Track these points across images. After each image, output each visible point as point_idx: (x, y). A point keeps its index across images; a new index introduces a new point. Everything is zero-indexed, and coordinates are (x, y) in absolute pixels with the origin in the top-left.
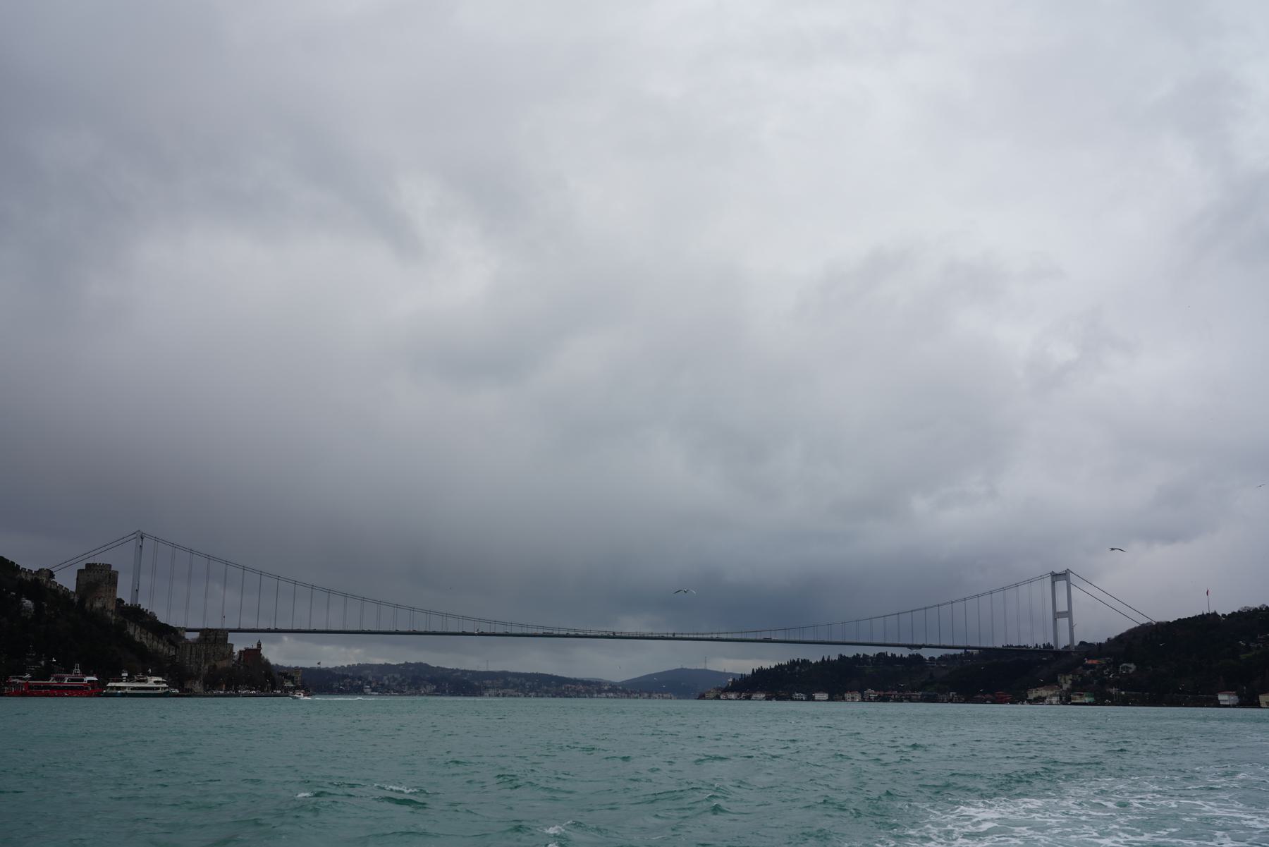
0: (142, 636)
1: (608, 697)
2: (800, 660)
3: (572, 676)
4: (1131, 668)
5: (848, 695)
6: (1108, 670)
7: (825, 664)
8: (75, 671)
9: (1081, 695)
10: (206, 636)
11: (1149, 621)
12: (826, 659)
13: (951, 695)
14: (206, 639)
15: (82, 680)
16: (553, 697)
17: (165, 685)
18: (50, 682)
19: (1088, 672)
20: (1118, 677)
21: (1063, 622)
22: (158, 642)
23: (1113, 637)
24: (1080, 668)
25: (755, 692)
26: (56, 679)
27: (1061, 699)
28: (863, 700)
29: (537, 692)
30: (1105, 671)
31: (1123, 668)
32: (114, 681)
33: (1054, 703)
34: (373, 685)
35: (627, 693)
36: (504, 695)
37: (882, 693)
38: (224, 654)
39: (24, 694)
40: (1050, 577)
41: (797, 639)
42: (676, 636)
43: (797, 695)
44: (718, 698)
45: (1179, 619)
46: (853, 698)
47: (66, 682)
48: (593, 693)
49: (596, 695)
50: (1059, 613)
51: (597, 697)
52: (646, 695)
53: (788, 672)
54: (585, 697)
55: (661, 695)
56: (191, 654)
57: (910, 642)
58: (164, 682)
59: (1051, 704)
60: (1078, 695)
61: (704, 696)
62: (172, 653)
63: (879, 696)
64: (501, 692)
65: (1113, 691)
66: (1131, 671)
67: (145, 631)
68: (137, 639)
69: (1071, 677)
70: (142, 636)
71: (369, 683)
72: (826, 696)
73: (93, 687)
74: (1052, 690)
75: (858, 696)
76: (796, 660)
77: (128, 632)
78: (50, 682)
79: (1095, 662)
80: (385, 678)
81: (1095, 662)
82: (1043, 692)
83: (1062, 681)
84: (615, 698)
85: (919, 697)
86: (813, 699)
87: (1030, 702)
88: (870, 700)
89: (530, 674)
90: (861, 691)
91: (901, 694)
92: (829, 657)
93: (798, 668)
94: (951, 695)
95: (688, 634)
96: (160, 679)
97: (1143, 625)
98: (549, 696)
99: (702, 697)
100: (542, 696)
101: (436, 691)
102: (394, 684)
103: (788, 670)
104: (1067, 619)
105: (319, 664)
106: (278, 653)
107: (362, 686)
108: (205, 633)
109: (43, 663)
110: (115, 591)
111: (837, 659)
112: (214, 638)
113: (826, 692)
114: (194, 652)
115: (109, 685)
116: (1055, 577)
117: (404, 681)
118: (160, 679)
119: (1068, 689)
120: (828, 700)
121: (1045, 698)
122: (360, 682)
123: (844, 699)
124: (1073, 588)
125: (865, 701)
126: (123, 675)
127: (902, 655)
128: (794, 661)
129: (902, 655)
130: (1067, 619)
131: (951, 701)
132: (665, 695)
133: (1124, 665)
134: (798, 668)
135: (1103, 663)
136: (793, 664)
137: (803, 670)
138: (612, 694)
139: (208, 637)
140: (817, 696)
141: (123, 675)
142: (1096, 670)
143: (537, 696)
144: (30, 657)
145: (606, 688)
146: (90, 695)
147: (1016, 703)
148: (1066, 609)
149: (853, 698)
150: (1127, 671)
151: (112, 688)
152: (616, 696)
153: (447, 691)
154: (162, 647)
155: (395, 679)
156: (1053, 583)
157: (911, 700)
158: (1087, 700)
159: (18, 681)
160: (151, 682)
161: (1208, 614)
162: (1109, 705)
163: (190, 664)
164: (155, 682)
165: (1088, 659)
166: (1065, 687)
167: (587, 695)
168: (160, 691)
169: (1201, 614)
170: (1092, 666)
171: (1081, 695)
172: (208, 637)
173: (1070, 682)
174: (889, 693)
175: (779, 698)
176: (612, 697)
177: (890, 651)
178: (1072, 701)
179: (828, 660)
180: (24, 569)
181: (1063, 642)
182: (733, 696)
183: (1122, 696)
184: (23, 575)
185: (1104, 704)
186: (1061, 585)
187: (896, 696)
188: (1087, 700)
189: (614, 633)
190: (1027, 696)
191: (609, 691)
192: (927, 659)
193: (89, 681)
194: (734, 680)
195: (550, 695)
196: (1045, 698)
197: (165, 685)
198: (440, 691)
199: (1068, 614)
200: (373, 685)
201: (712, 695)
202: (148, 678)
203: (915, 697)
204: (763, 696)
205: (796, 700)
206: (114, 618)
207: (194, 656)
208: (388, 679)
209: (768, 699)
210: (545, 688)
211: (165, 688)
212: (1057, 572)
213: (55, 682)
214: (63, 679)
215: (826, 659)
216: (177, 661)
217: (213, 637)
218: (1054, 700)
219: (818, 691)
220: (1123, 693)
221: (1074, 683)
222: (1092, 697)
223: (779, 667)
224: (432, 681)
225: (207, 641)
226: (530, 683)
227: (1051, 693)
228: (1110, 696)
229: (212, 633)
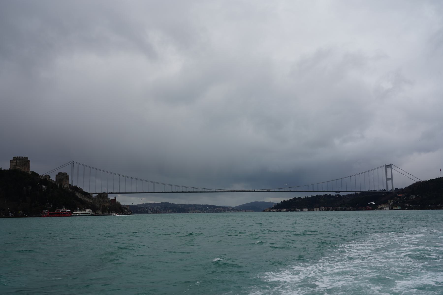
0: (81, 196)
1: (231, 212)
2: (298, 198)
3: (218, 205)
4: (413, 197)
5: (315, 209)
6: (406, 198)
7: (307, 199)
8: (63, 208)
9: (396, 206)
11: (420, 180)
12: (307, 197)
13: (351, 208)
14: (100, 197)
15: (66, 211)
16: (212, 212)
17: (92, 212)
18: (55, 212)
19: (399, 199)
20: (409, 200)
21: (390, 182)
22: (86, 198)
23: (407, 186)
24: (396, 197)
25: (283, 209)
26: (57, 211)
27: (389, 208)
28: (320, 210)
29: (207, 211)
30: (404, 198)
31: (411, 197)
32: (75, 211)
33: (387, 209)
34: (151, 210)
36: (196, 212)
37: (327, 208)
38: (107, 201)
39: (48, 216)
40: (385, 167)
41: (297, 190)
43: (297, 209)
44: (270, 211)
45: (431, 180)
46: (316, 210)
47: (61, 212)
48: (226, 211)
49: (227, 211)
50: (388, 179)
51: (227, 212)
52: (244, 211)
53: (294, 202)
54: (223, 212)
55: (249, 211)
56: (97, 202)
57: (336, 191)
58: (91, 211)
59: (386, 210)
60: (395, 206)
61: (265, 210)
62: (91, 201)
63: (326, 209)
64: (194, 211)
65: (408, 205)
66: (414, 198)
67: (81, 195)
68: (79, 197)
69: (393, 200)
70: (81, 196)
71: (150, 210)
72: (307, 210)
73: (69, 214)
74: (386, 205)
75: (318, 209)
76: (296, 198)
77: (76, 195)
78: (55, 212)
79: (401, 195)
80: (155, 208)
81: (401, 195)
82: (383, 206)
83: (390, 202)
84: (234, 212)
85: (340, 209)
86: (303, 211)
87: (379, 209)
88: (323, 211)
89: (204, 205)
90: (319, 207)
91: (333, 208)
92: (308, 196)
93: (297, 200)
94: (351, 208)
95: (260, 190)
96: (90, 210)
97: (418, 182)
98: (211, 212)
99: (264, 211)
100: (209, 212)
101: (173, 211)
102: (159, 209)
103: (294, 201)
104: (391, 181)
105: (132, 203)
106: (123, 200)
107: (147, 211)
108: (100, 194)
109: (51, 206)
110: (68, 182)
111: (310, 197)
112: (103, 196)
113: (307, 208)
115: (74, 212)
116: (387, 166)
117: (161, 208)
118: (90, 210)
119: (392, 205)
120: (308, 211)
121: (384, 208)
122: (147, 209)
123: (313, 210)
124: (393, 170)
125: (320, 211)
126: (78, 209)
127: (333, 195)
128: (295, 198)
129: (333, 195)
130: (391, 181)
131: (350, 210)
132: (251, 211)
133: (411, 196)
134: (297, 200)
135: (404, 195)
136: (295, 199)
137: (299, 201)
138: (232, 211)
139: (101, 196)
140: (304, 210)
141: (78, 209)
142: (401, 198)
143: (207, 212)
144: (47, 204)
146: (68, 216)
147: (373, 210)
148: (391, 178)
149: (316, 210)
150: (412, 198)
151: (75, 213)
152: (234, 211)
153: (176, 211)
154: (87, 200)
155: (158, 208)
156: (386, 168)
157: (336, 210)
158: (398, 208)
159: (46, 212)
160: (87, 211)
161: (441, 177)
162: (406, 210)
163: (97, 205)
164: (89, 211)
165: (399, 195)
166: (391, 204)
167: (224, 212)
168: (90, 214)
169: (438, 177)
170: (400, 197)
171: (396, 206)
172: (101, 196)
173: (392, 202)
174: (329, 208)
175: (291, 211)
176: (232, 212)
177: (329, 194)
178: (393, 209)
179: (308, 197)
180: (41, 175)
181: (390, 188)
182: (275, 210)
183: (411, 206)
184: (40, 177)
185: (404, 210)
186: (389, 169)
187: (332, 209)
188: (398, 208)
189: (234, 190)
190: (377, 208)
191: (232, 210)
192: (342, 196)
193: (68, 211)
194: (275, 205)
195: (211, 212)
196: (384, 208)
197: (92, 212)
198: (174, 212)
199: (391, 179)
200: (151, 210)
201: (268, 210)
202: (86, 210)
203: (338, 209)
204: (285, 210)
205: (297, 211)
206: (71, 190)
208: (156, 208)
209: (287, 211)
211: (92, 213)
212: (387, 164)
213: (57, 212)
214: (60, 211)
215: (307, 197)
216: (93, 204)
217: (103, 196)
218: (387, 208)
219: (304, 208)
220: (411, 205)
221: (394, 203)
222: (400, 207)
223: (291, 200)
224: (171, 208)
226: (204, 208)
227: (386, 206)
228: (407, 207)
229: (102, 194)
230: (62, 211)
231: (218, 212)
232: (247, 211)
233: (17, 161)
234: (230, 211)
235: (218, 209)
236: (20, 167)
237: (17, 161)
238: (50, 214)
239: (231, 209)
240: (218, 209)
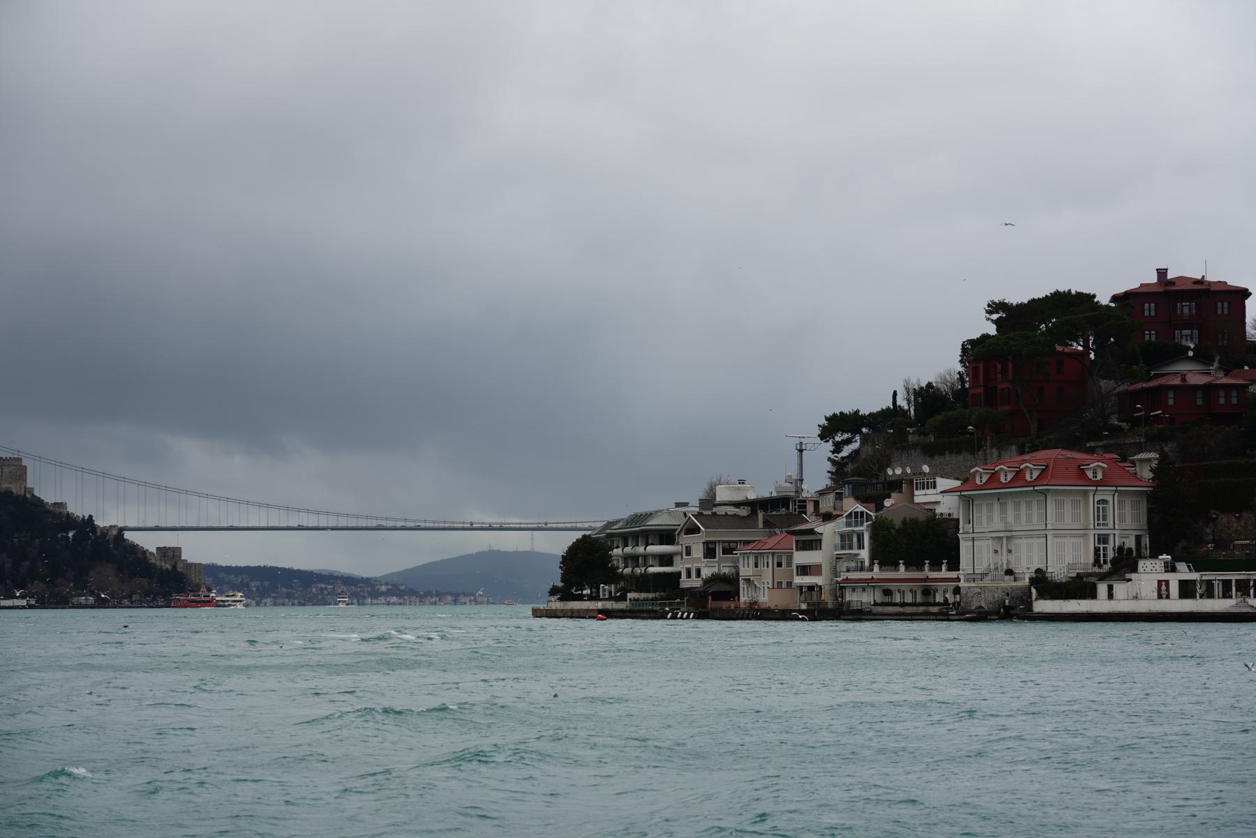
1: (388, 604)
10: (164, 553)
15: (209, 596)
16: (300, 604)
22: (165, 563)
35: (421, 597)
42: (549, 525)
48: (364, 598)
49: (369, 601)
51: (372, 604)
52: (450, 598)
55: (473, 598)
84: (400, 604)
98: (293, 604)
114: (197, 571)
138: (394, 599)
145: (384, 588)
152: (401, 601)
163: (196, 579)
167: (355, 601)
172: (166, 554)
176: (394, 604)
189: (472, 524)
191: (389, 593)
195: (296, 601)
207: (197, 574)
210: (284, 590)
217: (171, 554)
225: (166, 558)
226: (258, 583)
230: (204, 596)
231: (330, 604)
232: (463, 599)
233: (4, 467)
234: (382, 599)
235: (323, 586)
236: (9, 483)
237: (4, 467)
238: (189, 601)
239: (389, 590)
240: (323, 586)
